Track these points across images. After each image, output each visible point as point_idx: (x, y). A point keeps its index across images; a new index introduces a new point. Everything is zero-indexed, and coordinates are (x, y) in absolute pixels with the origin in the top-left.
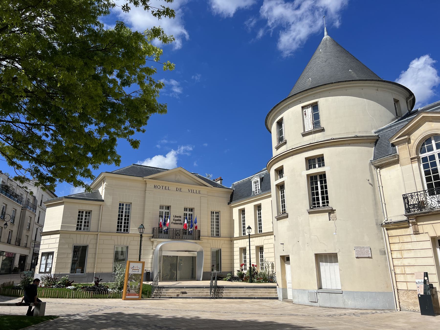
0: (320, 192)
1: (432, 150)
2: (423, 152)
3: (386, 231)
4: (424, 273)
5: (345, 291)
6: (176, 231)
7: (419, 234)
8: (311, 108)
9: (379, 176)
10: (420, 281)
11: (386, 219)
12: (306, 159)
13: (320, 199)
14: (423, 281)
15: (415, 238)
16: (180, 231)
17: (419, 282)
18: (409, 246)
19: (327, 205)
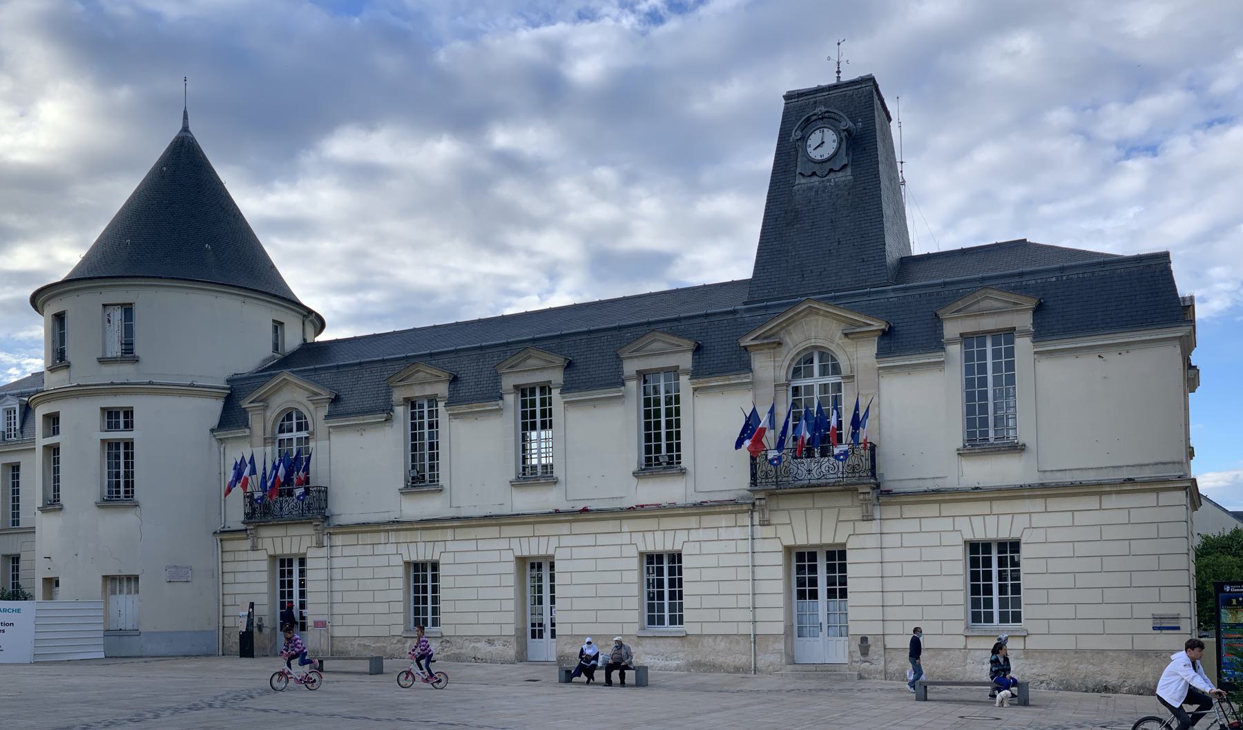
0: (122, 473)
1: (291, 431)
2: (281, 431)
9: (222, 455)
19: (132, 497)
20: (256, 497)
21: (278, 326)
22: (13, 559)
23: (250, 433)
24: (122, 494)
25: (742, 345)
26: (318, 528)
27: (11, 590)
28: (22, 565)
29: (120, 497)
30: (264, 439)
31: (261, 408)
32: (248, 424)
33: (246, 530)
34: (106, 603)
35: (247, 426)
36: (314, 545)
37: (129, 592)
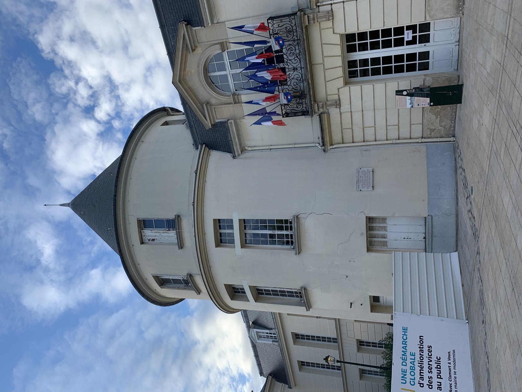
3: (334, 147)
4: (396, 95)
5: (428, 212)
7: (339, 99)
8: (144, 231)
9: (255, 148)
10: (408, 102)
11: (317, 145)
12: (217, 246)
13: (280, 232)
14: (408, 98)
15: (345, 107)
17: (410, 104)
18: (357, 117)
20: (285, 102)
22: (360, 345)
23: (232, 119)
24: (289, 232)
26: (311, 16)
27: (383, 349)
28: (365, 339)
29: (292, 235)
30: (235, 103)
32: (225, 122)
33: (320, 116)
34: (396, 250)
35: (226, 122)
36: (329, 24)
37: (385, 229)
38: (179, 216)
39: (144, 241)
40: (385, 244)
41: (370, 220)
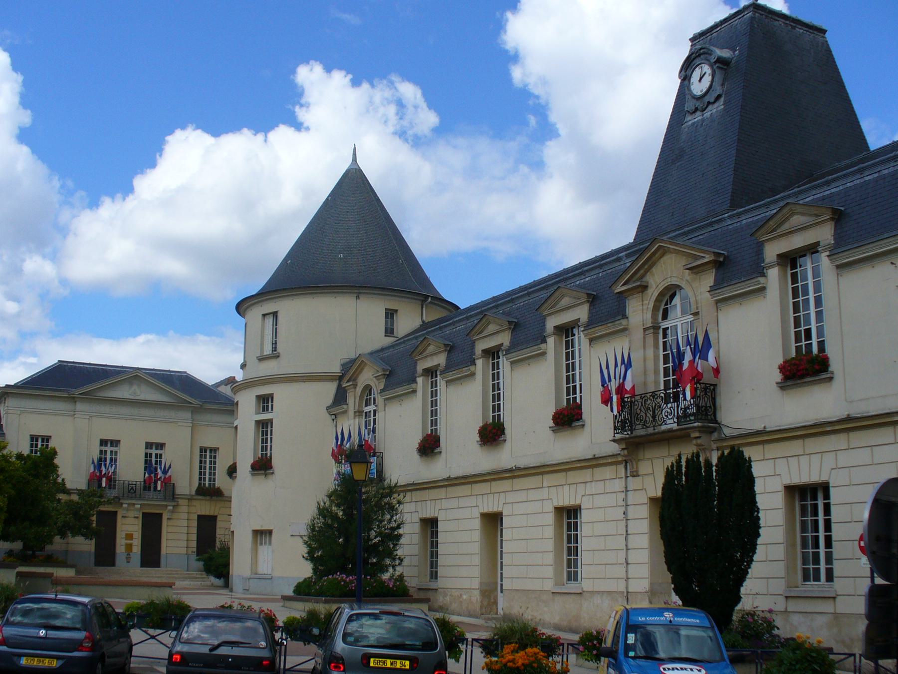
6: (129, 484)
16: (136, 484)
21: (390, 314)
25: (616, 291)
31: (352, 386)
32: (346, 401)
38: (279, 356)
39: (266, 316)
40: (261, 544)
41: (270, 532)
